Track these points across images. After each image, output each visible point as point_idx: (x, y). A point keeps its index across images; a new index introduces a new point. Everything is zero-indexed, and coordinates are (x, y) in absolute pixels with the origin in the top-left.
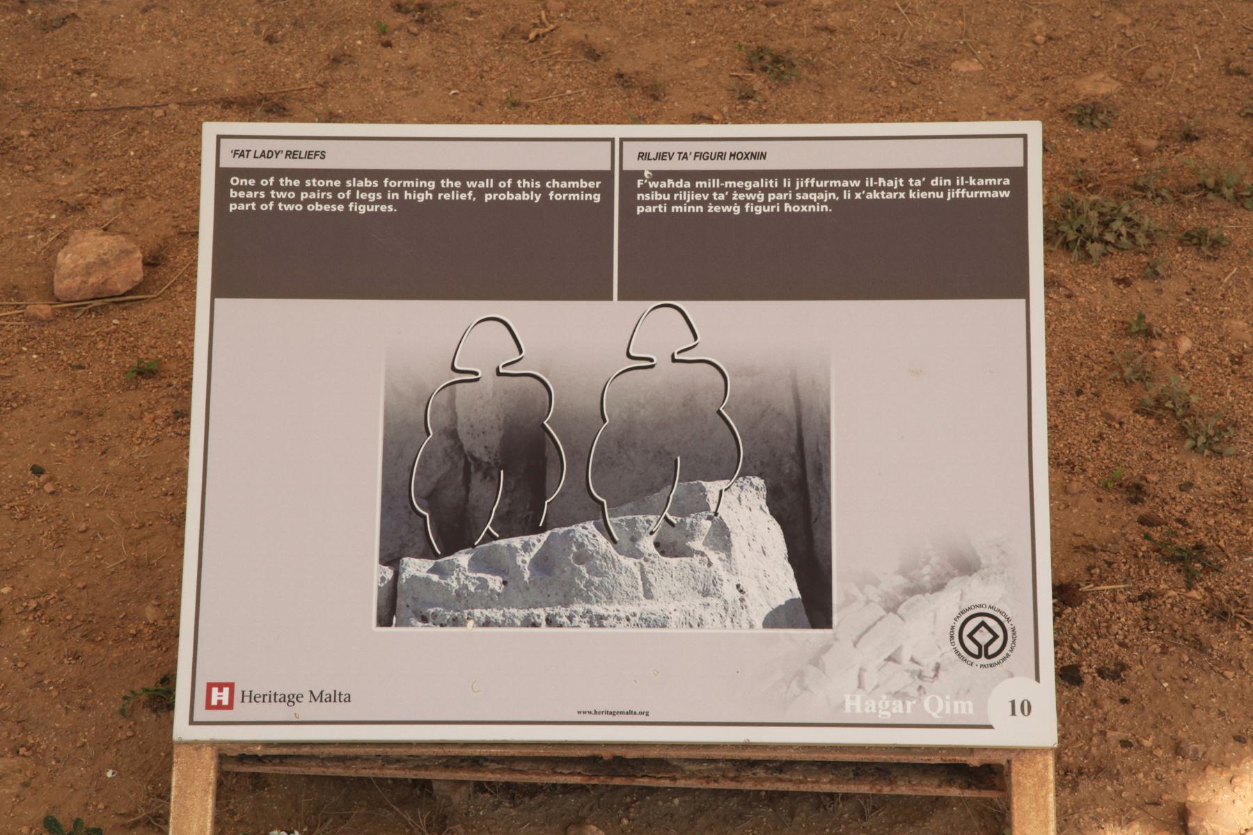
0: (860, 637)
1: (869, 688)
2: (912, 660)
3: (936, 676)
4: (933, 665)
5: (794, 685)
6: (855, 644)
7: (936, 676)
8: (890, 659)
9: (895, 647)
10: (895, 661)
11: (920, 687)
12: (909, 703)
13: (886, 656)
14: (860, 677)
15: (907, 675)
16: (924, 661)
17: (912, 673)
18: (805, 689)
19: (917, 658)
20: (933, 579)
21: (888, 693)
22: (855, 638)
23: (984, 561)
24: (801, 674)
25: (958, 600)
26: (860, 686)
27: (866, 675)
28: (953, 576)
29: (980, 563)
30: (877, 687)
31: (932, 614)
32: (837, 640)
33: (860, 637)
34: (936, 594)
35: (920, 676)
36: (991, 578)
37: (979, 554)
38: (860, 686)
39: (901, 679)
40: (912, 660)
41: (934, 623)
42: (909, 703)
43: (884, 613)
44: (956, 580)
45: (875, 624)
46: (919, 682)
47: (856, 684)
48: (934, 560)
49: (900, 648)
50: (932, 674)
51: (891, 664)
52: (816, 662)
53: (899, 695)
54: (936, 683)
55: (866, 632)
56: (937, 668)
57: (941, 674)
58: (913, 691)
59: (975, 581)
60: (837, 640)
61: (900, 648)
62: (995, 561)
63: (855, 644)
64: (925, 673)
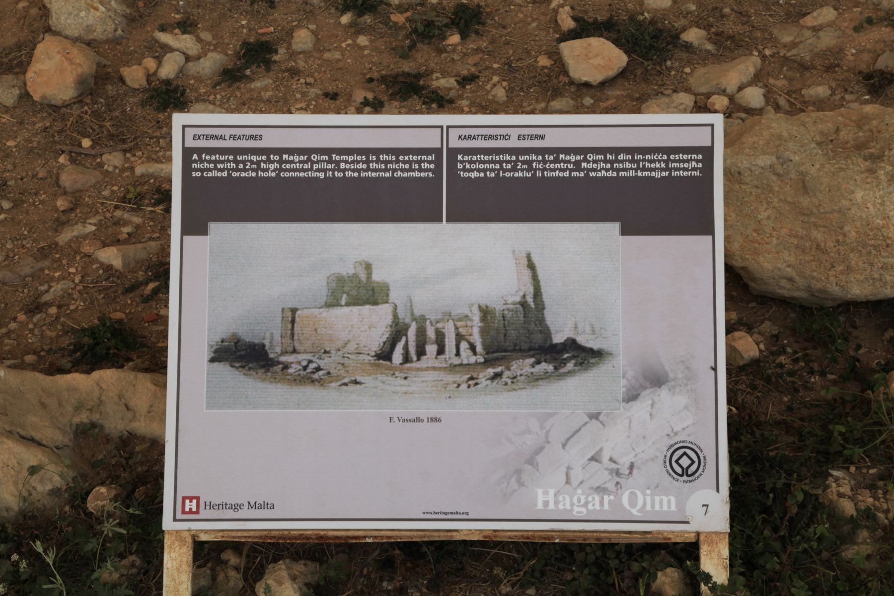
0: (568, 439)
1: (575, 483)
2: (611, 460)
3: (630, 473)
4: (627, 465)
5: (513, 480)
6: (564, 448)
7: (630, 473)
8: (593, 459)
9: (597, 449)
10: (596, 461)
11: (618, 483)
12: (606, 498)
13: (589, 456)
14: (567, 475)
15: (607, 472)
16: (621, 461)
17: (611, 471)
18: (521, 484)
19: (615, 457)
20: (628, 390)
21: (591, 488)
22: (563, 440)
23: (671, 375)
24: (518, 472)
25: (649, 408)
26: (568, 482)
27: (573, 473)
28: (645, 388)
29: (668, 377)
30: (582, 482)
31: (628, 420)
32: (548, 442)
33: (568, 439)
34: (631, 403)
35: (618, 473)
36: (677, 390)
37: (667, 368)
38: (568, 482)
39: (604, 478)
40: (611, 460)
41: (630, 428)
42: (606, 498)
43: (587, 419)
44: (648, 391)
45: (580, 429)
46: (618, 480)
47: (564, 480)
48: (630, 374)
49: (601, 450)
50: (627, 472)
51: (593, 463)
52: (531, 461)
53: (600, 490)
54: (631, 480)
55: (572, 436)
56: (632, 467)
57: (635, 471)
58: (611, 486)
59: (664, 392)
60: (548, 442)
61: (601, 450)
62: (680, 375)
63: (564, 446)
64: (621, 471)
